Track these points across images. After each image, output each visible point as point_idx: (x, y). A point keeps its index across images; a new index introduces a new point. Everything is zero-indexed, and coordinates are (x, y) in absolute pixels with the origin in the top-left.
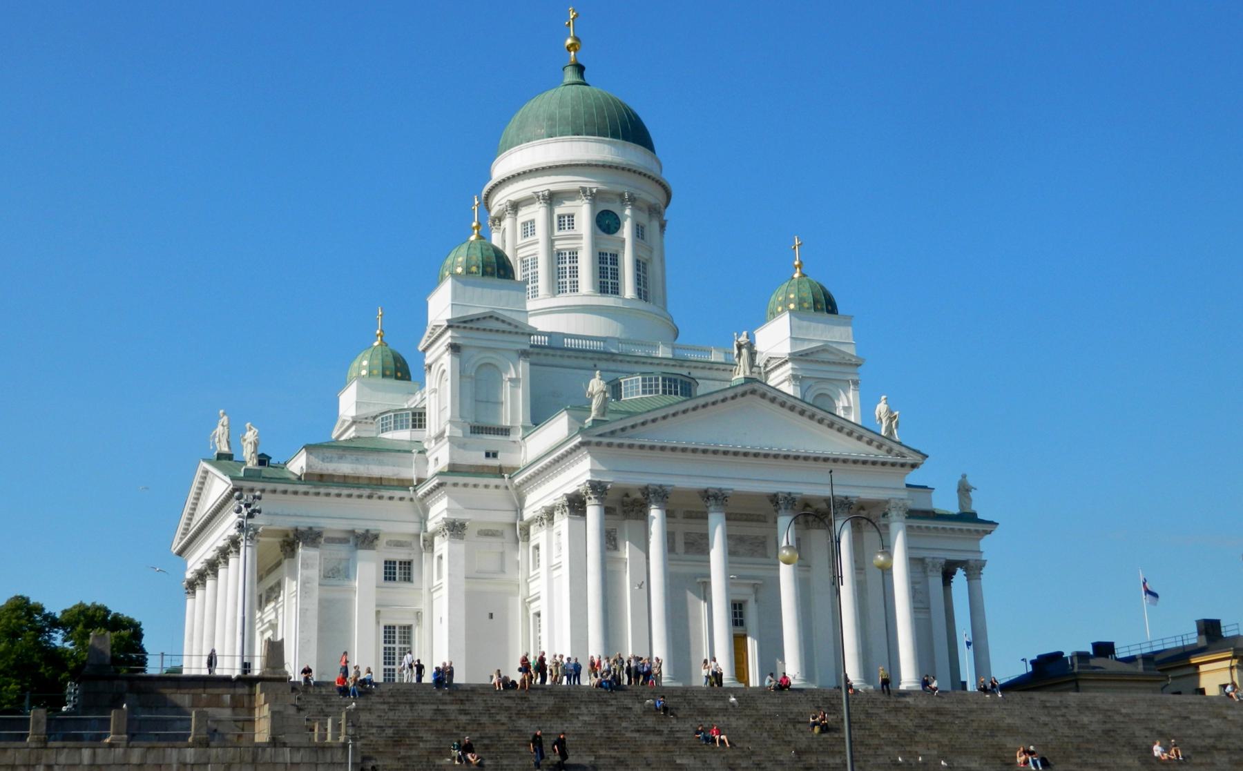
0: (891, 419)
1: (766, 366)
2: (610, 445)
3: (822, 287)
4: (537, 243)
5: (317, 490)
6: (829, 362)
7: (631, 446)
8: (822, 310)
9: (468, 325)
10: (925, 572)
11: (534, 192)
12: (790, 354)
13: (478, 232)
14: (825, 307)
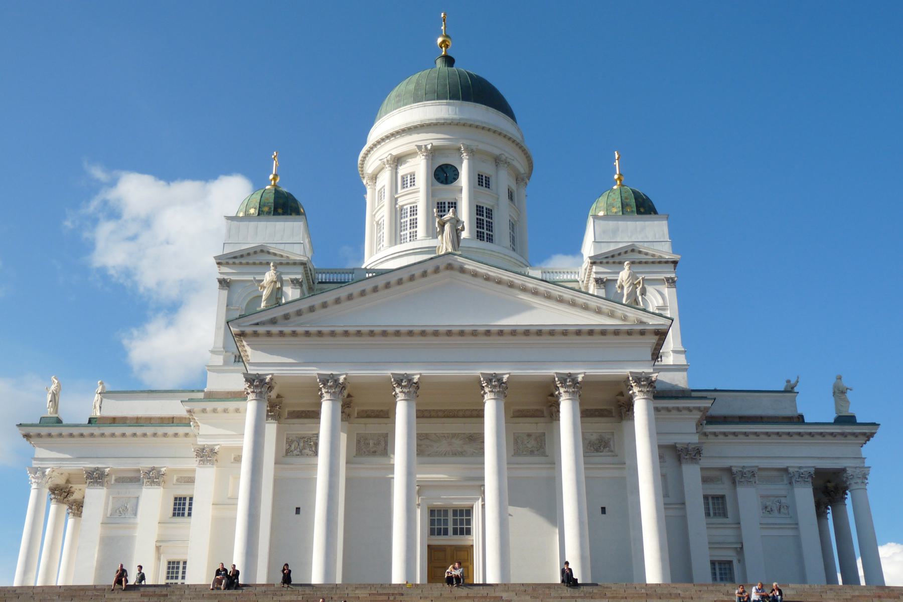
0: (635, 286)
1: (583, 281)
2: (269, 334)
3: (634, 192)
4: (383, 206)
5: (102, 432)
6: (640, 263)
7: (294, 334)
8: (632, 212)
9: (237, 261)
10: (791, 483)
11: (380, 160)
12: (590, 258)
13: (275, 183)
14: (635, 209)
